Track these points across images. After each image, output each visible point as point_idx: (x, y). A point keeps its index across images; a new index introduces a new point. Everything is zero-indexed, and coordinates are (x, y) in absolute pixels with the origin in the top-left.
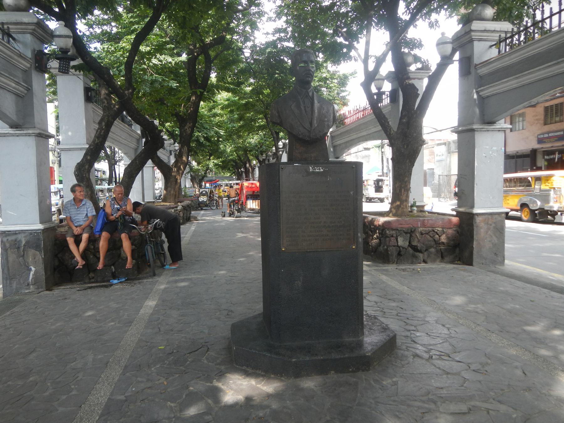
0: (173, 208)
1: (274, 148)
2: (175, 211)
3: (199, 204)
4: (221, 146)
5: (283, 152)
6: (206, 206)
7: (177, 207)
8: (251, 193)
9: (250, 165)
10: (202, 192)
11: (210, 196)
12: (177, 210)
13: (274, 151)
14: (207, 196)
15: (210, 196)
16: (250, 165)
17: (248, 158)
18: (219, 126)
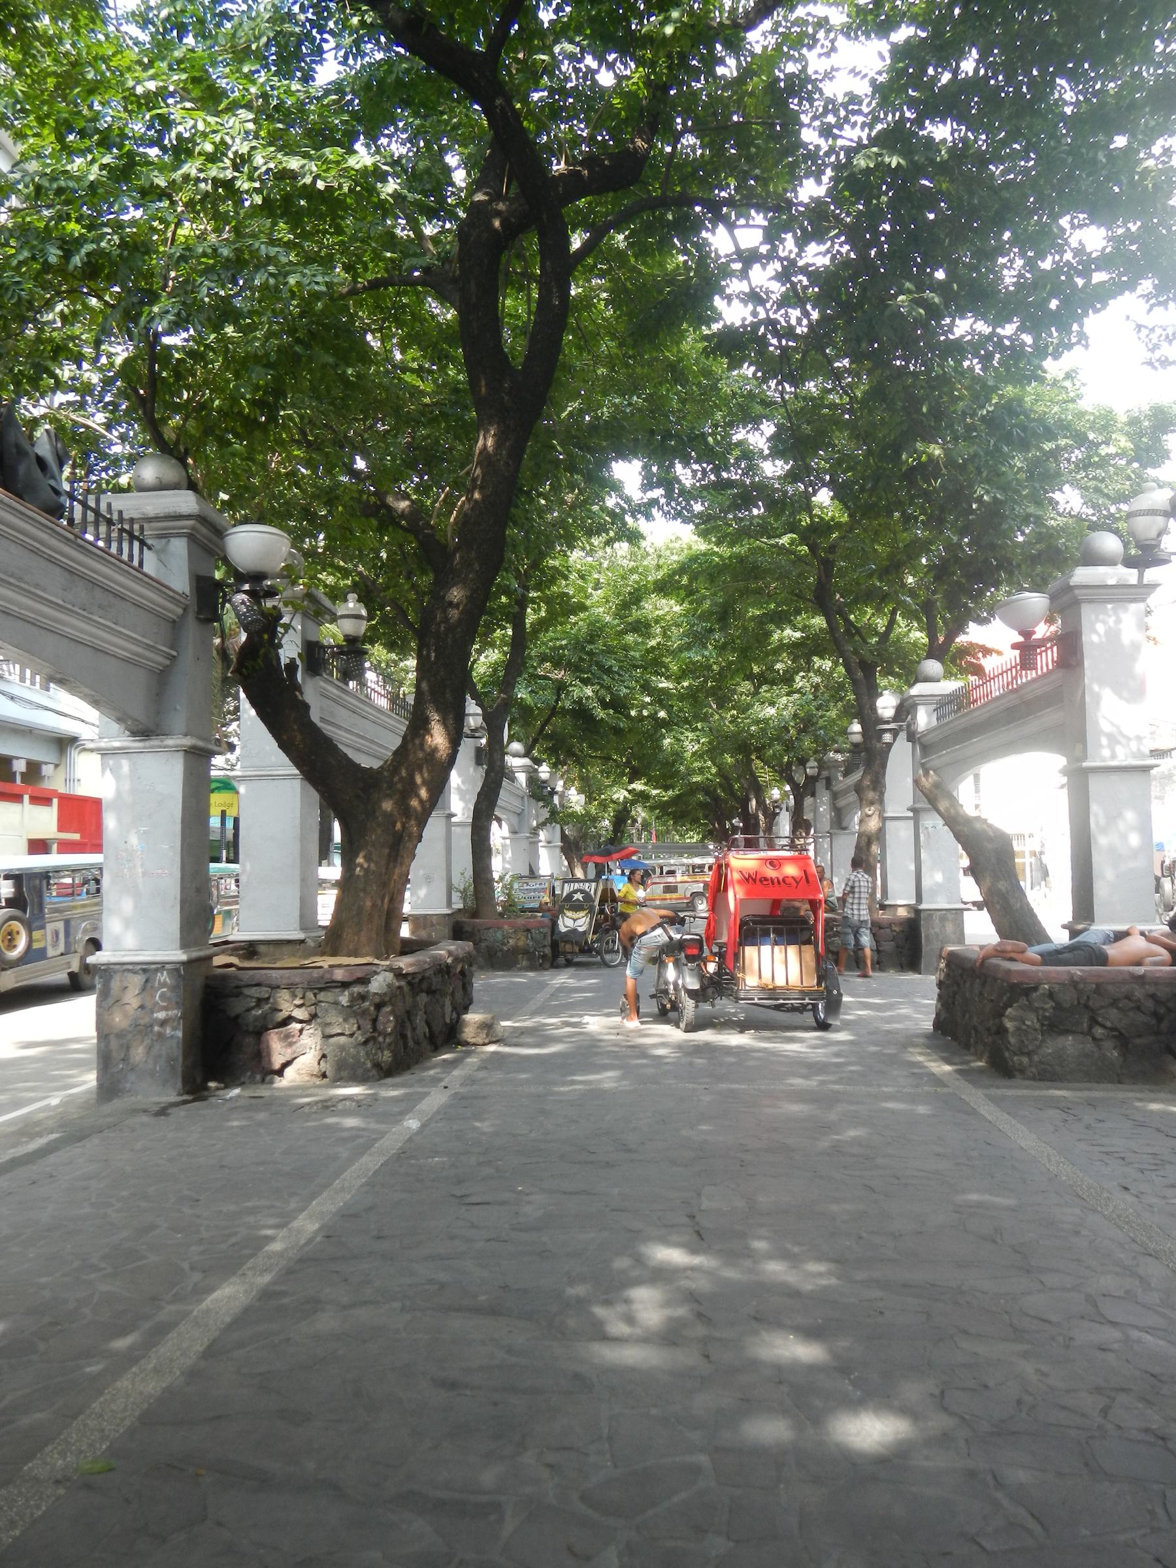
0: (345, 985)
1: (856, 727)
2: (353, 999)
3: (555, 945)
4: (667, 742)
5: (895, 733)
6: (586, 950)
7: (364, 981)
8: (761, 908)
9: (761, 803)
10: (570, 896)
11: (602, 911)
12: (363, 997)
13: (857, 738)
14: (591, 910)
15: (602, 911)
16: (761, 803)
17: (754, 778)
18: (654, 662)
